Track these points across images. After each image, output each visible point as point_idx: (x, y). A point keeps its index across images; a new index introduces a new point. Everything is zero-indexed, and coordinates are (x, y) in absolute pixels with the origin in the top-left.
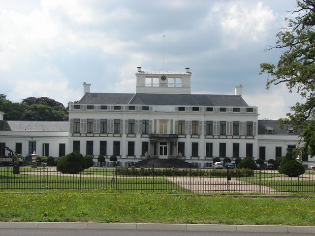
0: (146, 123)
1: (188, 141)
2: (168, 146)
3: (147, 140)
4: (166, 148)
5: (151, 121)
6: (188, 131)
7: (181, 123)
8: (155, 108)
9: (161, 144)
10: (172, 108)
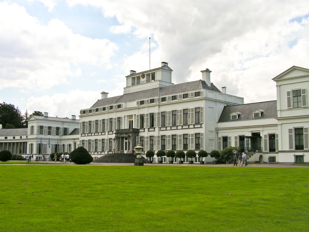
0: (119, 119)
1: (145, 134)
6: (147, 124)
7: (142, 117)
9: (126, 139)
10: (134, 104)
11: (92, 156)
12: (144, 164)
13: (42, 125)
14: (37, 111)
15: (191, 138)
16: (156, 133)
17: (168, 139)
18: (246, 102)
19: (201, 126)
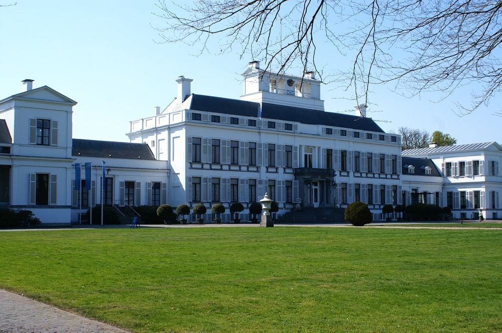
0: (289, 150)
2: (318, 187)
3: (290, 177)
4: (316, 190)
5: (296, 148)
8: (301, 127)
10: (319, 129)
11: (371, 211)
12: (275, 225)
13: (44, 115)
14: (444, 133)
15: (390, 190)
16: (352, 180)
17: (378, 189)
18: (86, 126)
19: (277, 170)
